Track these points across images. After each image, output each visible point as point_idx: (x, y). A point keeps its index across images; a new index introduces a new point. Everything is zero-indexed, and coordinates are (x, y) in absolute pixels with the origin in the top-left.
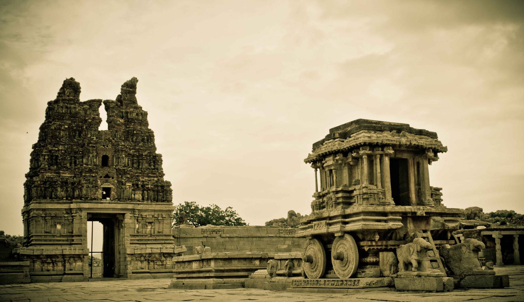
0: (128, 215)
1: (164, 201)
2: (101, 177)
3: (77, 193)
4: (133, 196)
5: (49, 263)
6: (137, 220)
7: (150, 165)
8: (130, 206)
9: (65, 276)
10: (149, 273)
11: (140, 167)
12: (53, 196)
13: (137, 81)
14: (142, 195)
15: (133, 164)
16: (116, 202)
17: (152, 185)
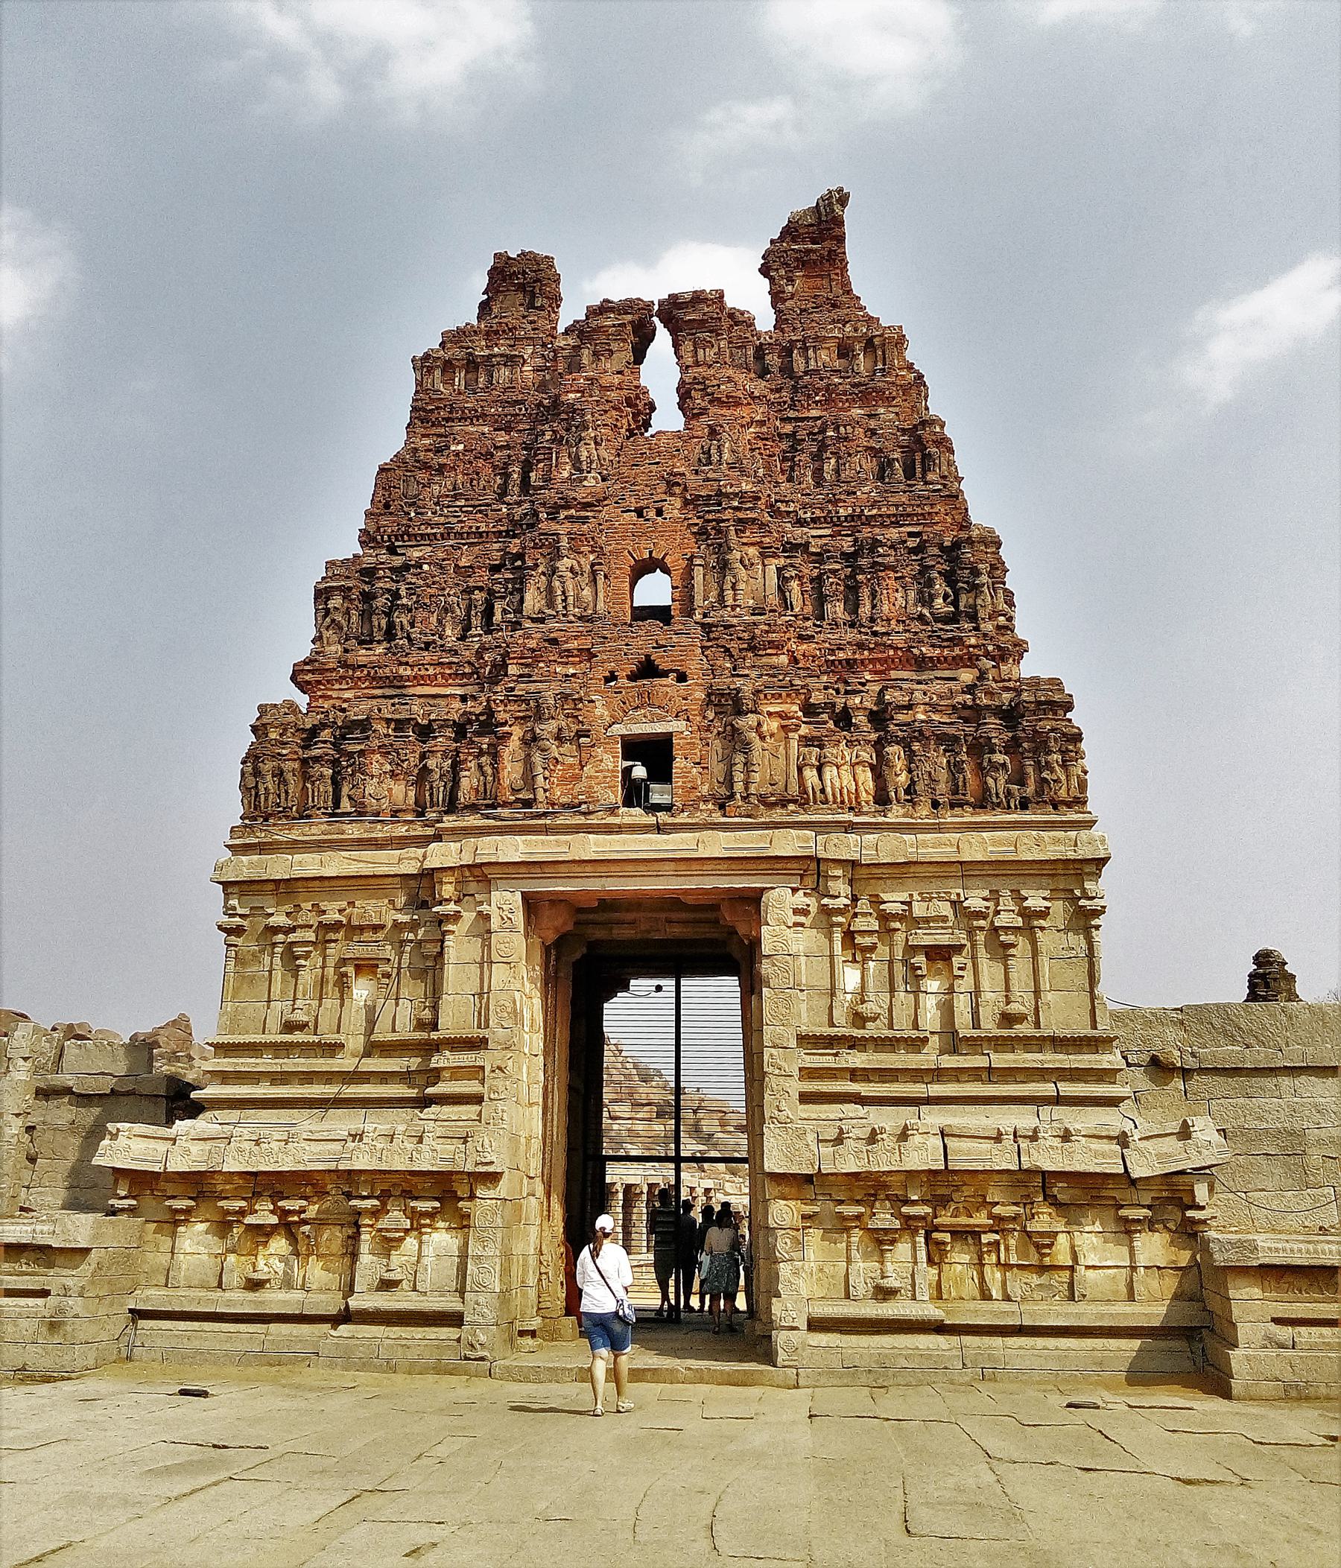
0: (783, 901)
1: (1024, 805)
2: (612, 677)
3: (469, 781)
4: (811, 775)
5: (261, 1233)
6: (849, 936)
7: (926, 600)
8: (789, 843)
9: (344, 1329)
10: (940, 1328)
11: (865, 610)
12: (346, 805)
13: (843, 200)
14: (879, 770)
15: (821, 600)
16: (699, 818)
17: (934, 708)
